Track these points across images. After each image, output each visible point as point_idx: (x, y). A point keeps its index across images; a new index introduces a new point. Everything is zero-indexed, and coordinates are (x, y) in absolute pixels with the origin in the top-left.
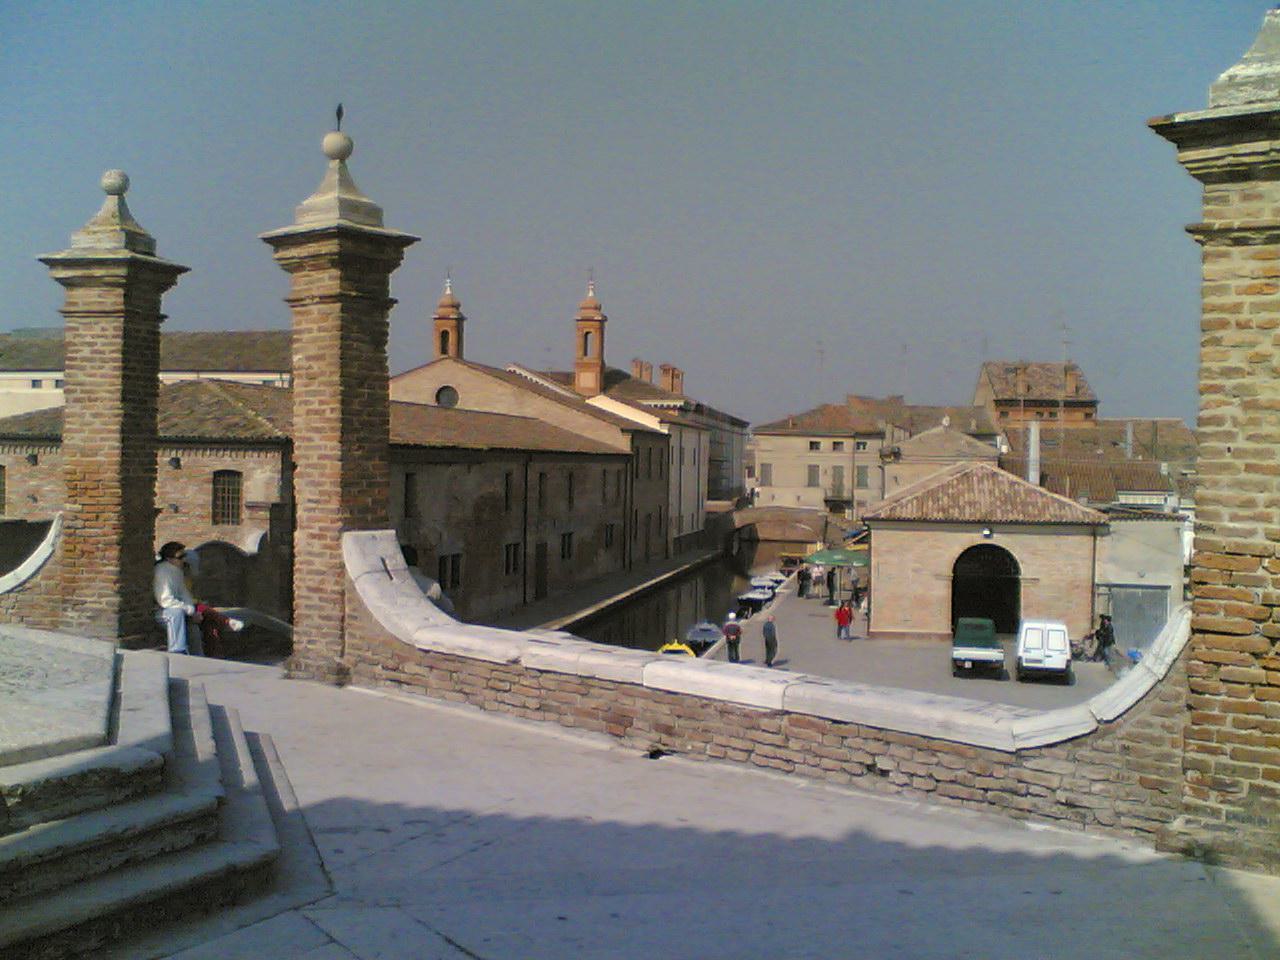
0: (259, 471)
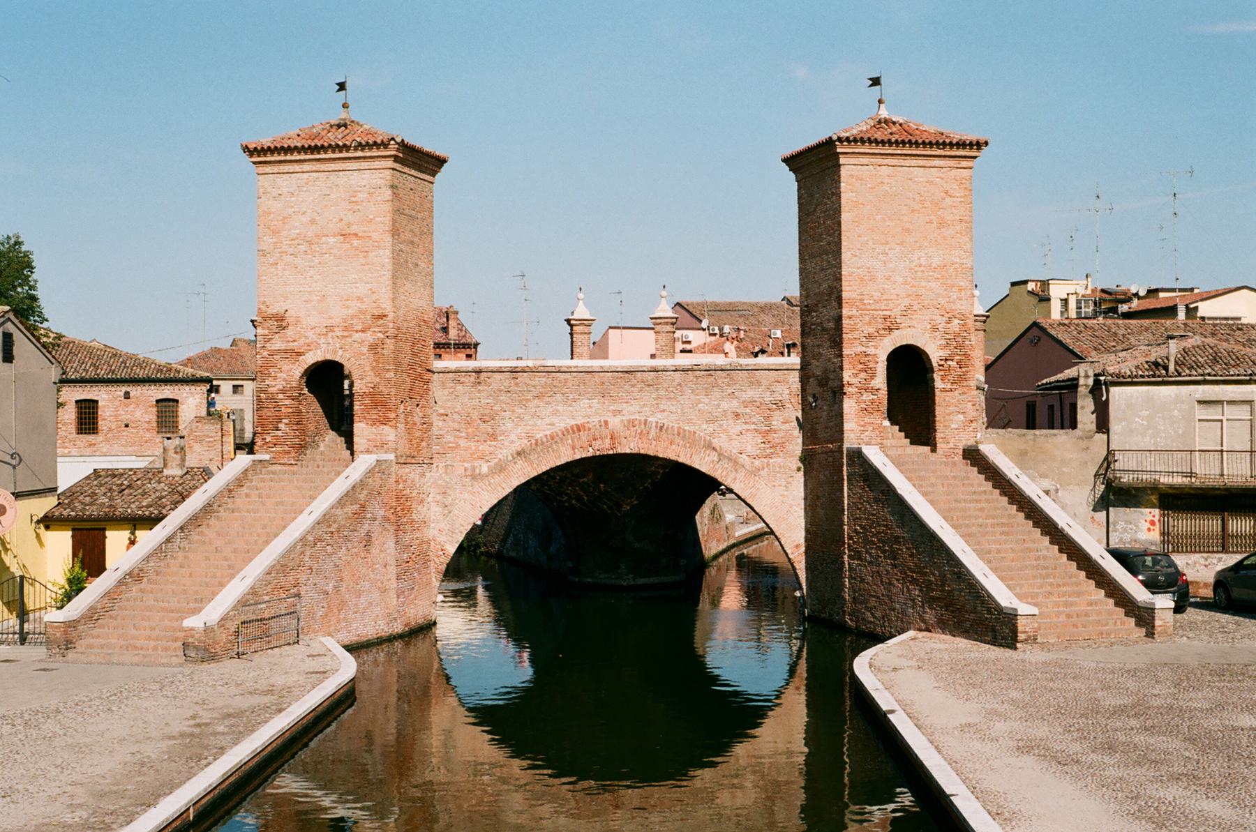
0: (191, 399)
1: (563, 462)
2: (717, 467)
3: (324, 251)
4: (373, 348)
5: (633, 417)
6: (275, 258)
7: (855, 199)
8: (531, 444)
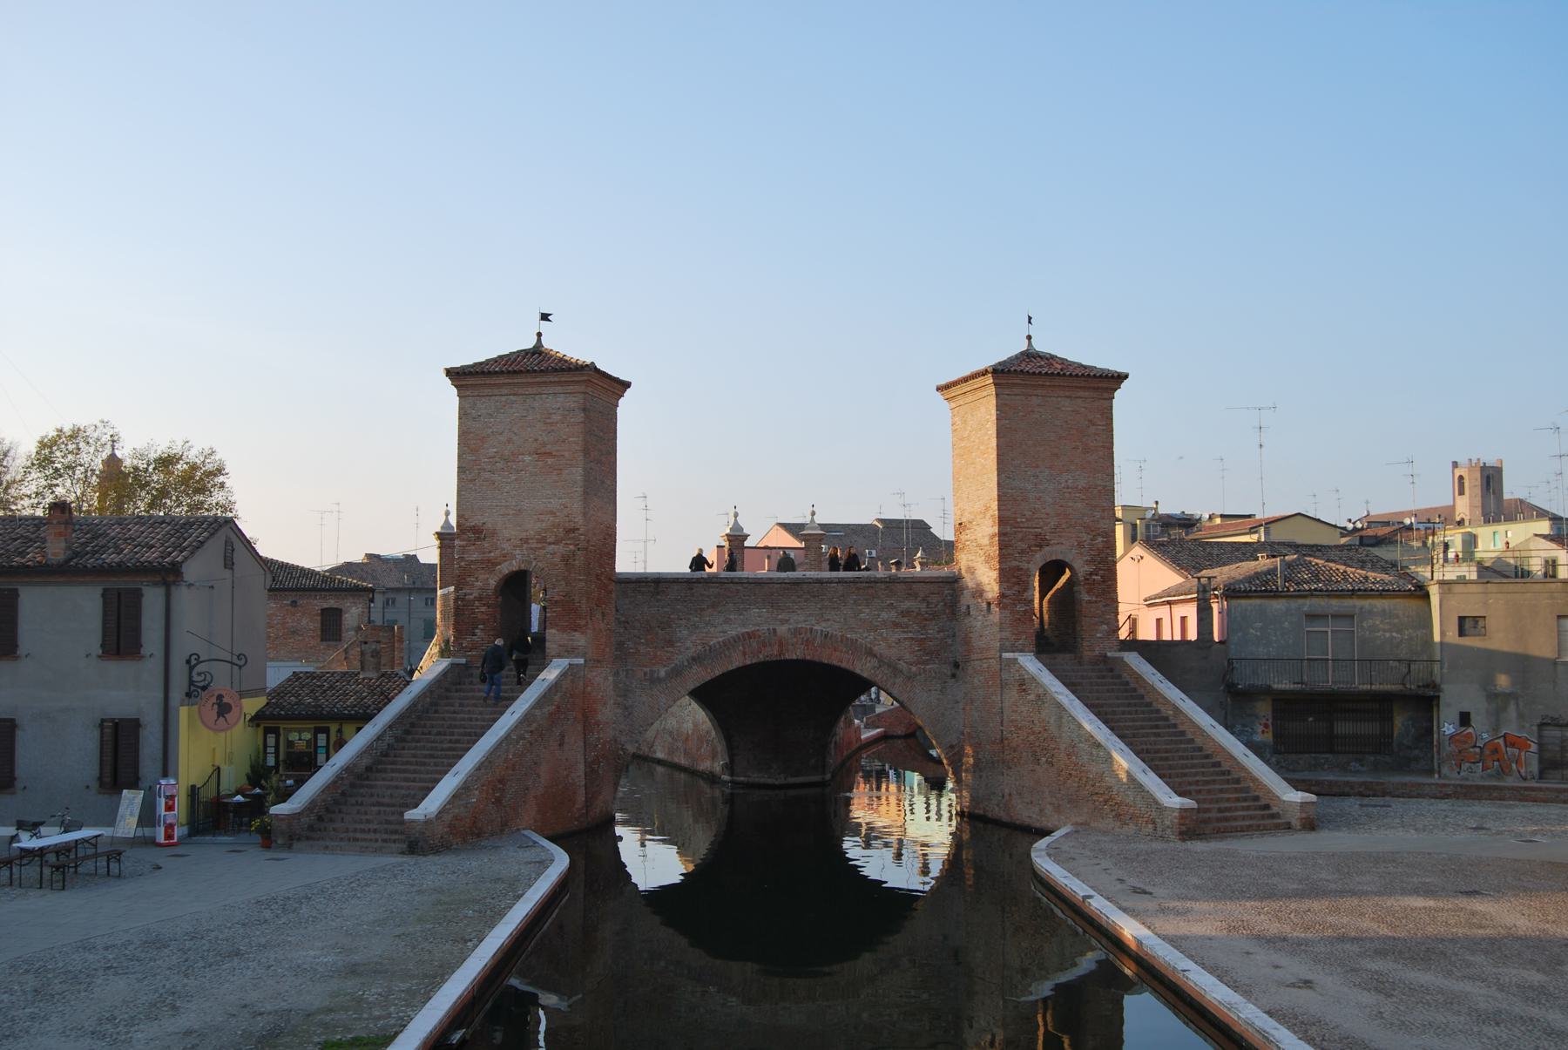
0: (354, 608)
1: (734, 667)
2: (878, 672)
3: (520, 469)
4: (567, 560)
5: (799, 626)
6: (473, 474)
7: (1008, 426)
8: (705, 650)
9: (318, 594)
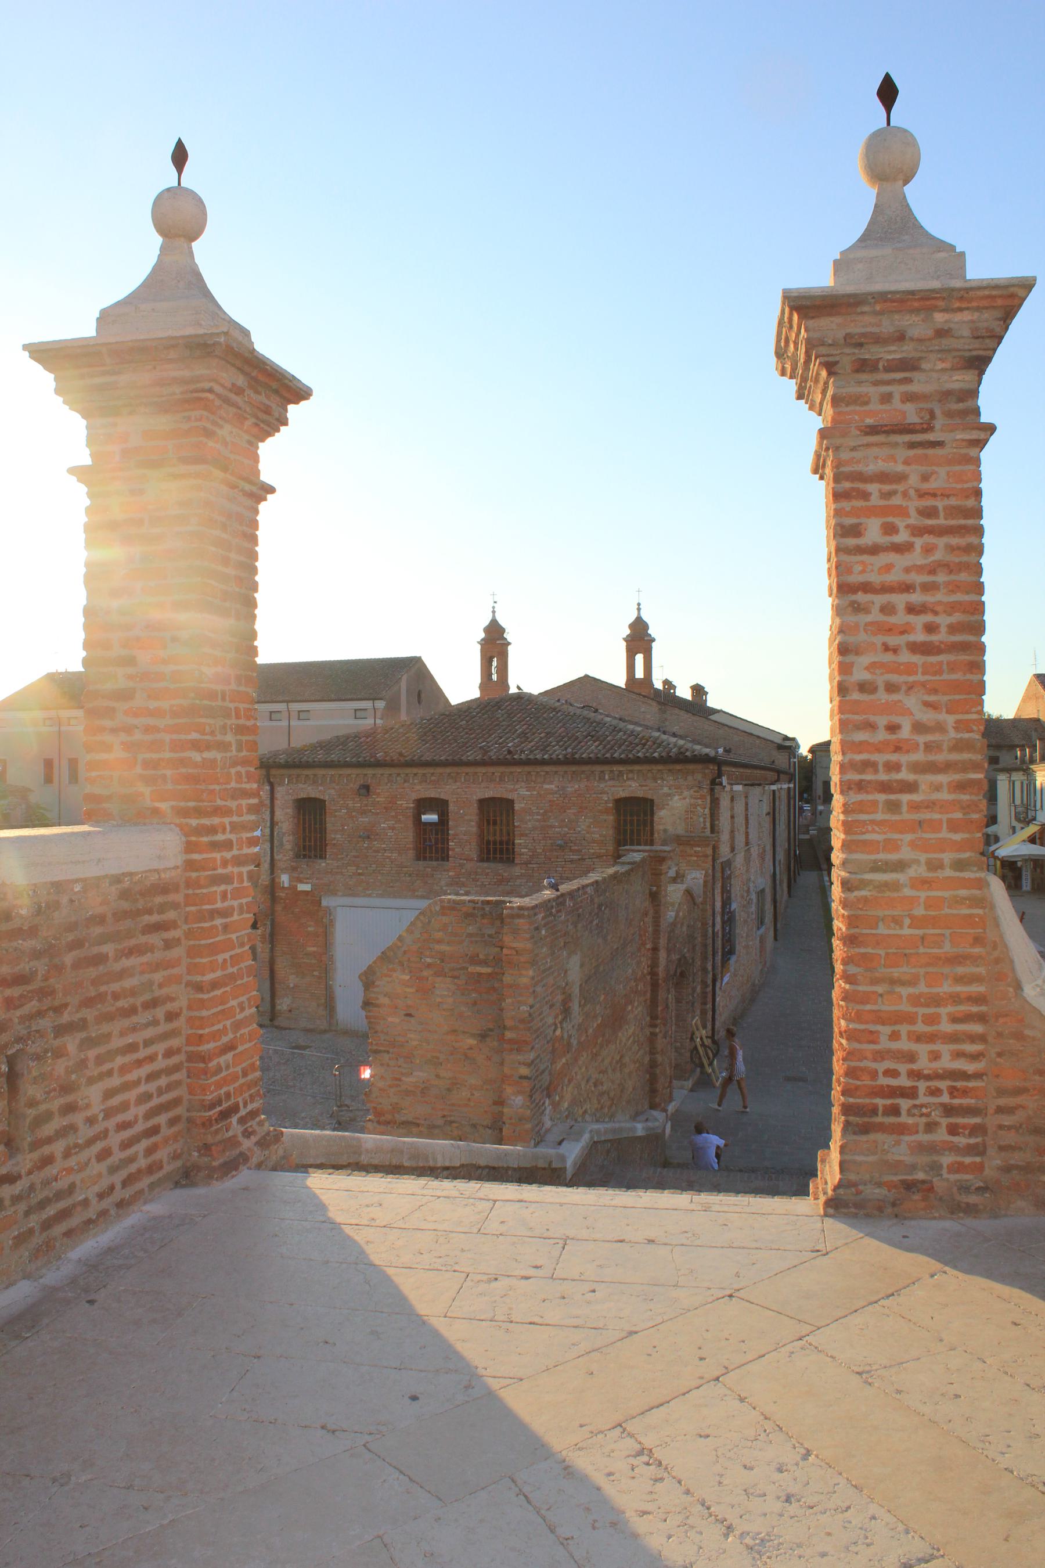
0: (676, 798)
9: (606, 768)
